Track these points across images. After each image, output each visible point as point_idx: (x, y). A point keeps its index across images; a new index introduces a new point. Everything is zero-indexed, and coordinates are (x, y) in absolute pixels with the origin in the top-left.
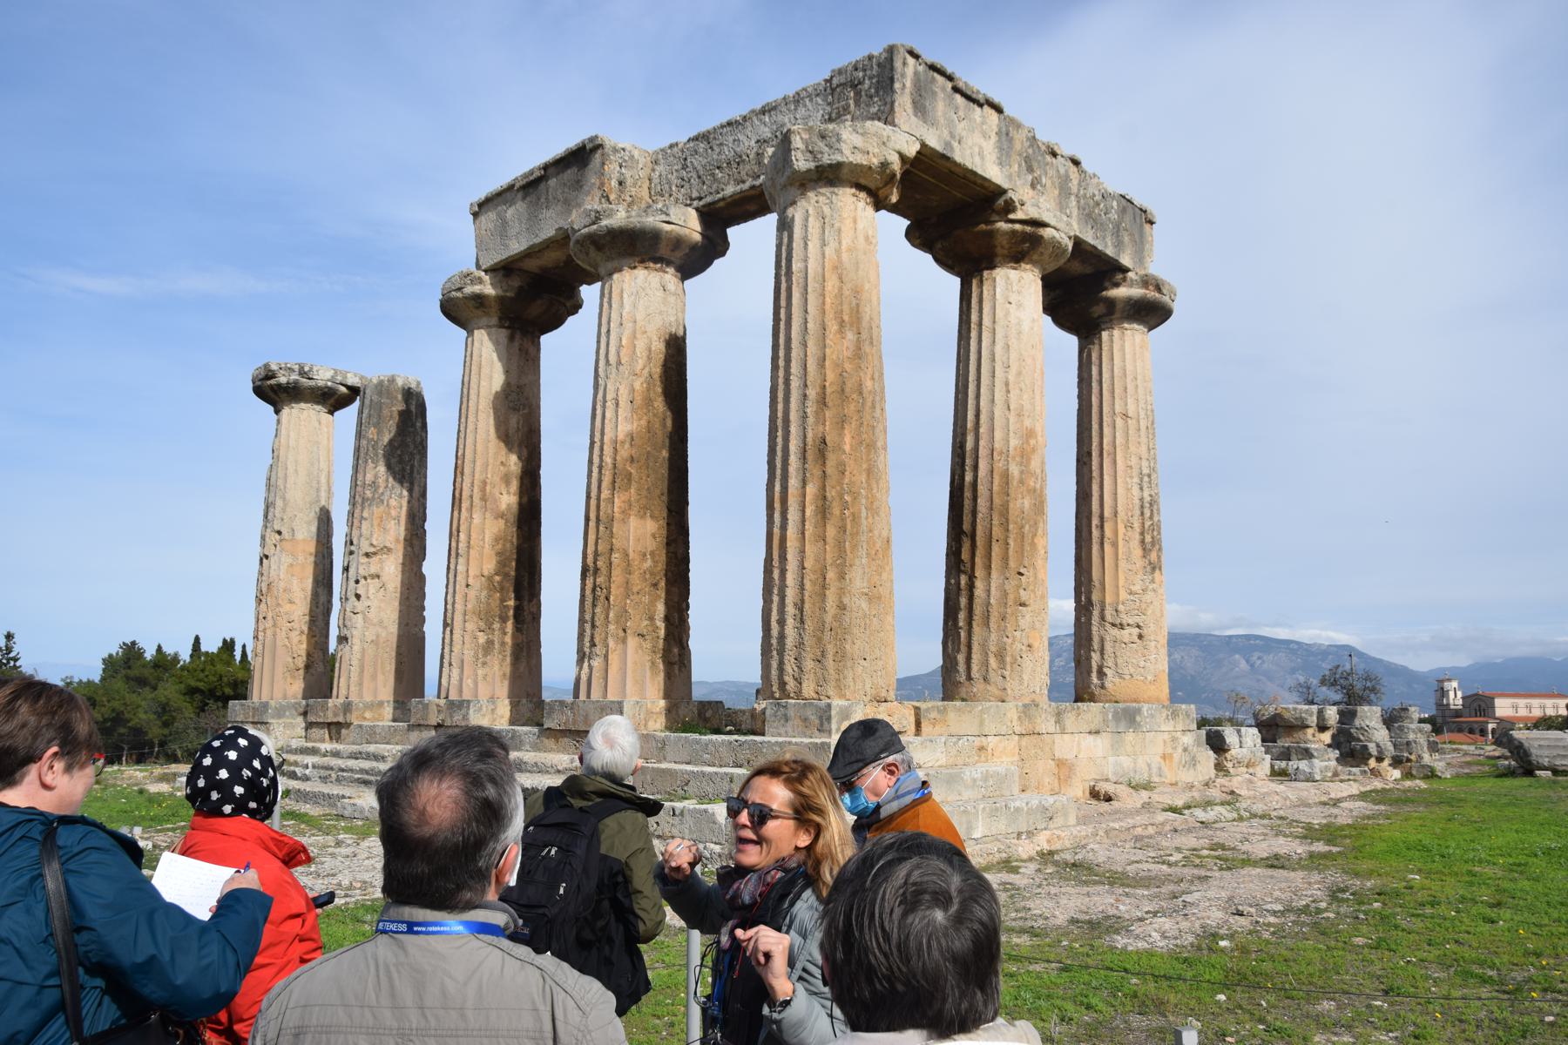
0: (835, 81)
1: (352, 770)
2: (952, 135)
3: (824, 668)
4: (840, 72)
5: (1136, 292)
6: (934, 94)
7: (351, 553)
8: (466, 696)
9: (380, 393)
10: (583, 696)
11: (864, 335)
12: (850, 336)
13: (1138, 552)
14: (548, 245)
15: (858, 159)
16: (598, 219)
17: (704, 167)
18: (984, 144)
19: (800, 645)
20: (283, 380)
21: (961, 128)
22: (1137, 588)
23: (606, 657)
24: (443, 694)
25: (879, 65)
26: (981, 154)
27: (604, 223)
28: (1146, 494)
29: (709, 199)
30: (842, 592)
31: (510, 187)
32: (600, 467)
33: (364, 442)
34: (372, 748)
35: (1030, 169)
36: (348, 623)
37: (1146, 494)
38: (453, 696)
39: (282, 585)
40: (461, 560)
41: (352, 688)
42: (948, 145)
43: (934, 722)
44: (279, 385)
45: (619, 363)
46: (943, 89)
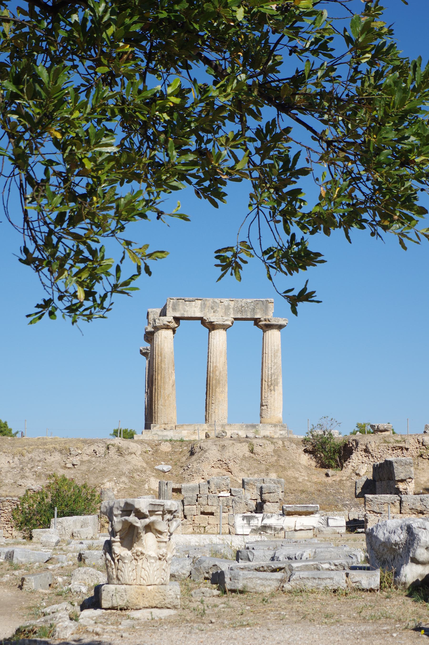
2: (184, 311)
5: (264, 323)
6: (179, 305)
11: (163, 357)
12: (160, 358)
13: (266, 387)
15: (159, 325)
18: (195, 309)
20: (144, 351)
21: (187, 309)
22: (266, 396)
26: (194, 312)
28: (270, 373)
30: (158, 404)
35: (212, 308)
37: (270, 373)
42: (184, 314)
43: (180, 428)
46: (182, 302)
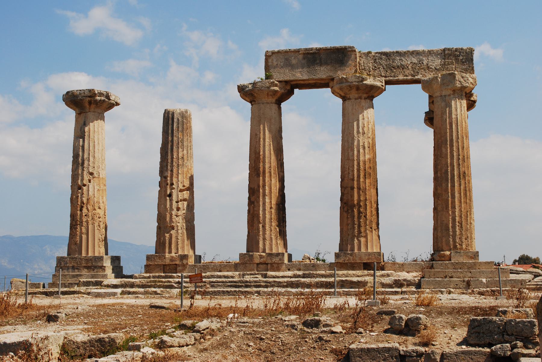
0: (446, 52)
1: (223, 282)
3: (468, 241)
4: (449, 49)
7: (174, 188)
8: (274, 251)
9: (183, 117)
10: (356, 251)
14: (313, 79)
16: (362, 81)
17: (386, 65)
19: (461, 234)
20: (98, 98)
23: (366, 237)
24: (261, 250)
25: (466, 53)
27: (365, 82)
29: (391, 78)
31: (297, 51)
32: (359, 170)
33: (175, 139)
34: (219, 274)
36: (174, 220)
38: (267, 251)
39: (96, 200)
40: (267, 197)
41: (179, 249)
44: (96, 101)
45: (364, 133)
